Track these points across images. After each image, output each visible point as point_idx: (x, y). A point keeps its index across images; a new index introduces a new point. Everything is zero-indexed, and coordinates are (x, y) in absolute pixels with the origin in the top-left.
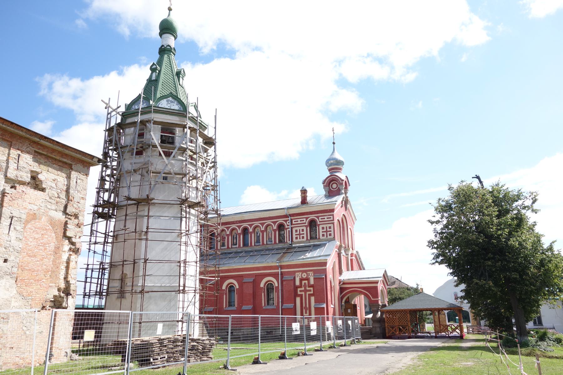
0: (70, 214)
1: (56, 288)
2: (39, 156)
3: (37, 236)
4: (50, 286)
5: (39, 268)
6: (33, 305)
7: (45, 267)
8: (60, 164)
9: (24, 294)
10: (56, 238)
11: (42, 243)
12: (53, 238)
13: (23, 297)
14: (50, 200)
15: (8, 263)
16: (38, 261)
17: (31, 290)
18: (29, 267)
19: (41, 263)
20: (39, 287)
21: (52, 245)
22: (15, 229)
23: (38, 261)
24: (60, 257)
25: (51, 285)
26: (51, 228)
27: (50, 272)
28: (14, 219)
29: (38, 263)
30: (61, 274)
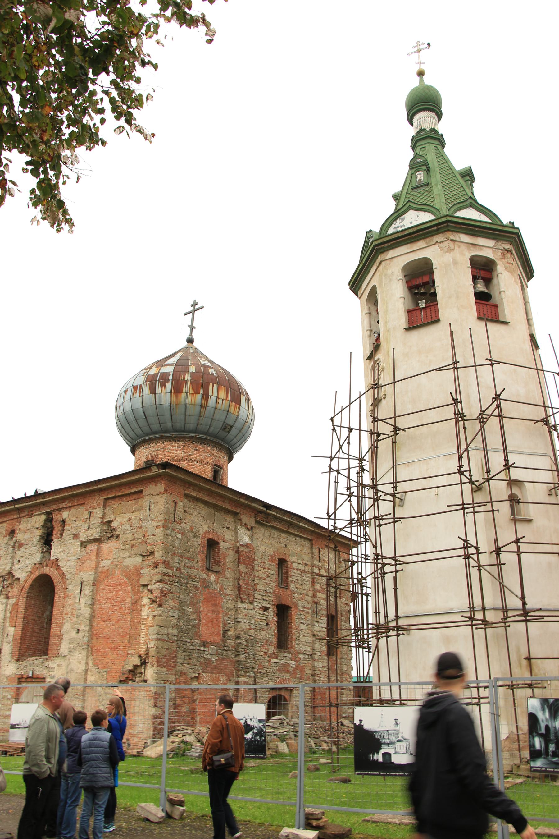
0: (144, 554)
1: (137, 656)
2: (113, 502)
3: (109, 596)
4: (128, 654)
5: (115, 633)
6: (109, 679)
7: (121, 630)
8: (135, 497)
9: (99, 666)
10: (133, 590)
11: (116, 602)
12: (128, 592)
13: (98, 670)
14: (124, 547)
15: (80, 633)
16: (113, 625)
17: (107, 660)
18: (105, 633)
19: (117, 626)
20: (116, 656)
21: (128, 600)
22: (84, 594)
23: (113, 625)
24: (139, 614)
25: (129, 652)
26: (127, 580)
27: (128, 636)
28: (85, 583)
29: (113, 627)
30: (142, 636)
